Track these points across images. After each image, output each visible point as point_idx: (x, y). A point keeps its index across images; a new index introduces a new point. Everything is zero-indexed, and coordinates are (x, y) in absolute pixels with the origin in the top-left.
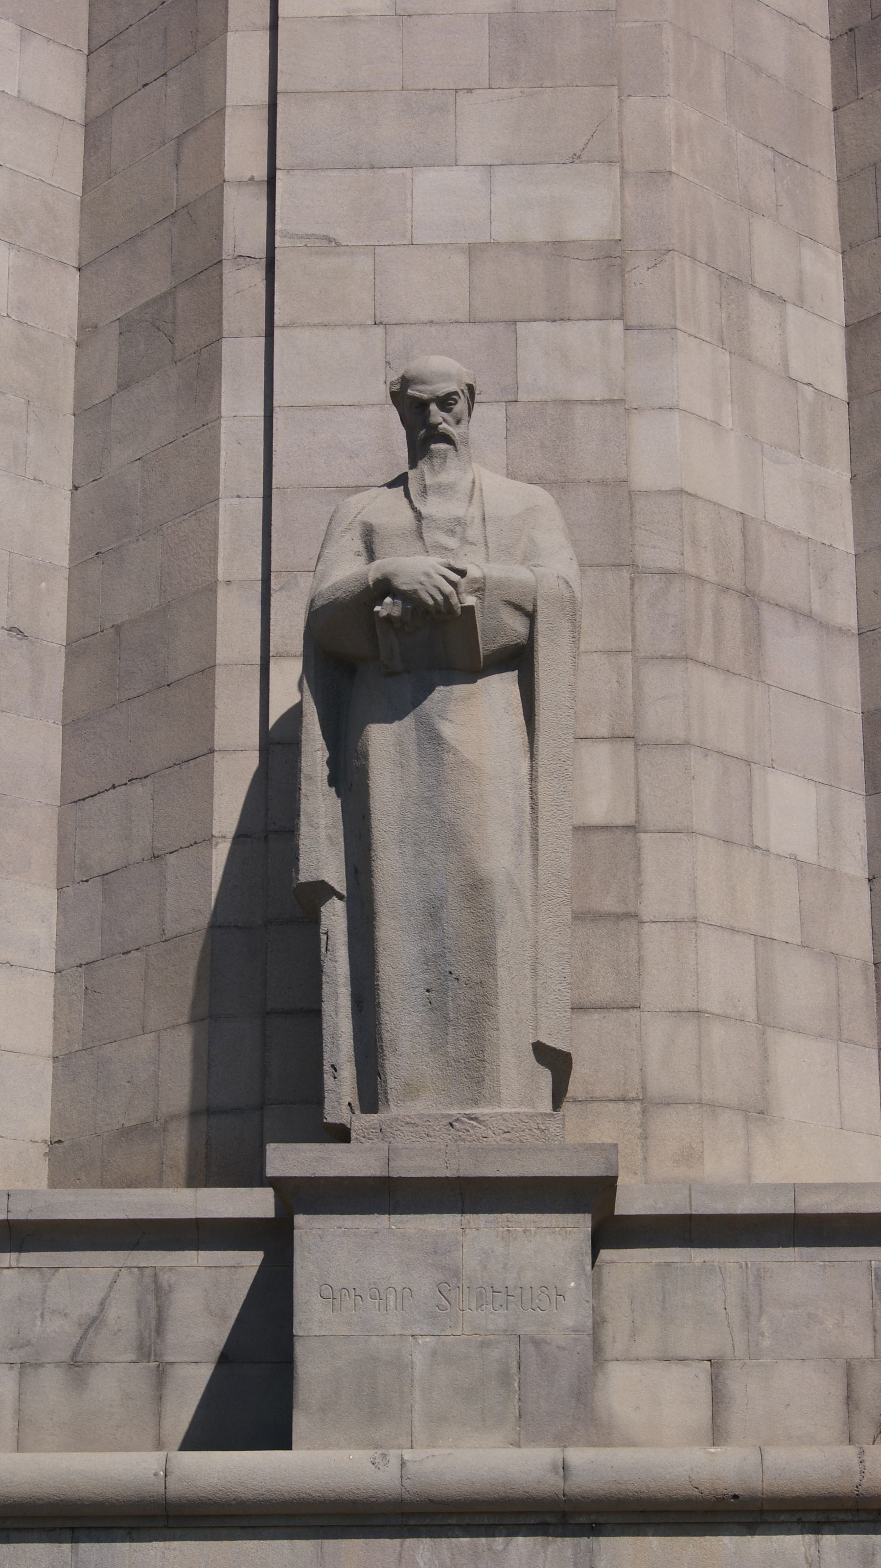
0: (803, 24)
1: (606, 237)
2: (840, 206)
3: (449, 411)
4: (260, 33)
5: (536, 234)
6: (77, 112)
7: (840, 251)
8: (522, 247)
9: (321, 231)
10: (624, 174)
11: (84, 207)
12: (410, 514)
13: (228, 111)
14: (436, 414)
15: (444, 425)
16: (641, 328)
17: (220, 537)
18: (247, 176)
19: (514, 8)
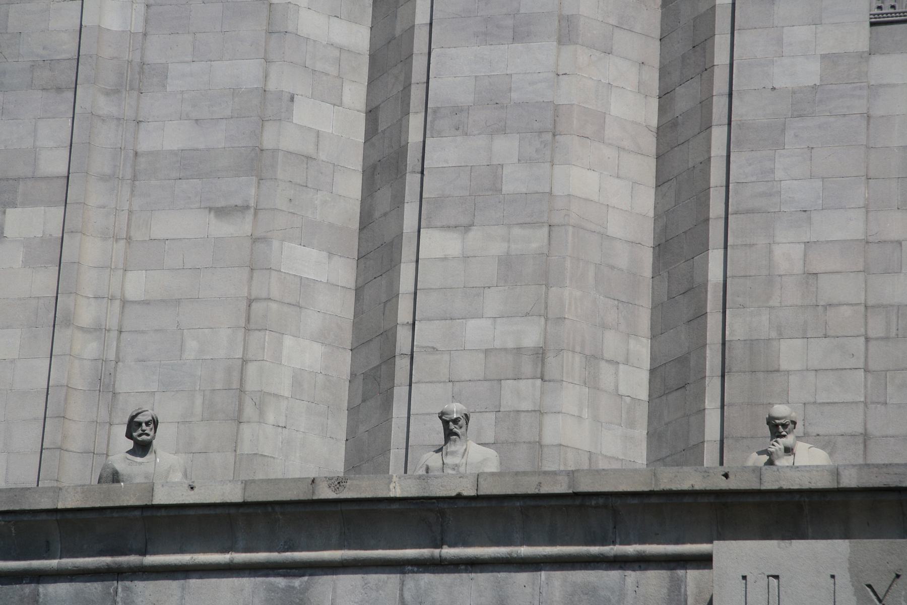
0: (639, 243)
1: (537, 346)
2: (651, 319)
3: (457, 424)
4: (413, 263)
5: (511, 345)
6: (352, 284)
7: (650, 338)
8: (506, 349)
9: (431, 345)
10: (547, 319)
11: (354, 324)
12: (442, 462)
13: (400, 295)
14: (452, 426)
15: (455, 429)
16: (550, 381)
17: (391, 464)
18: (407, 321)
19: (508, 253)
